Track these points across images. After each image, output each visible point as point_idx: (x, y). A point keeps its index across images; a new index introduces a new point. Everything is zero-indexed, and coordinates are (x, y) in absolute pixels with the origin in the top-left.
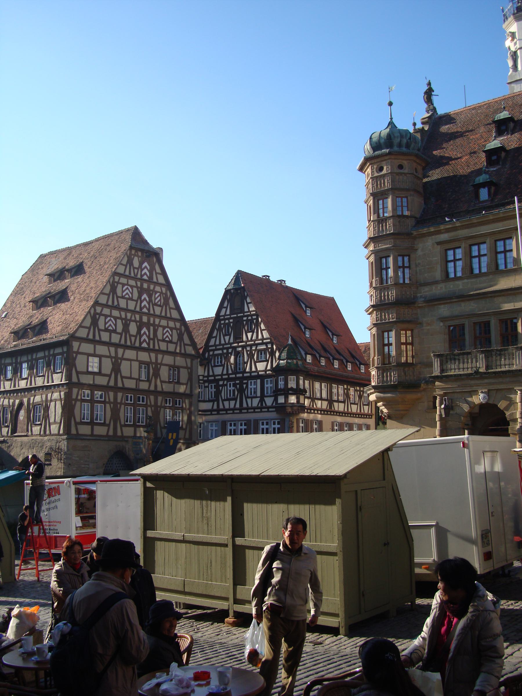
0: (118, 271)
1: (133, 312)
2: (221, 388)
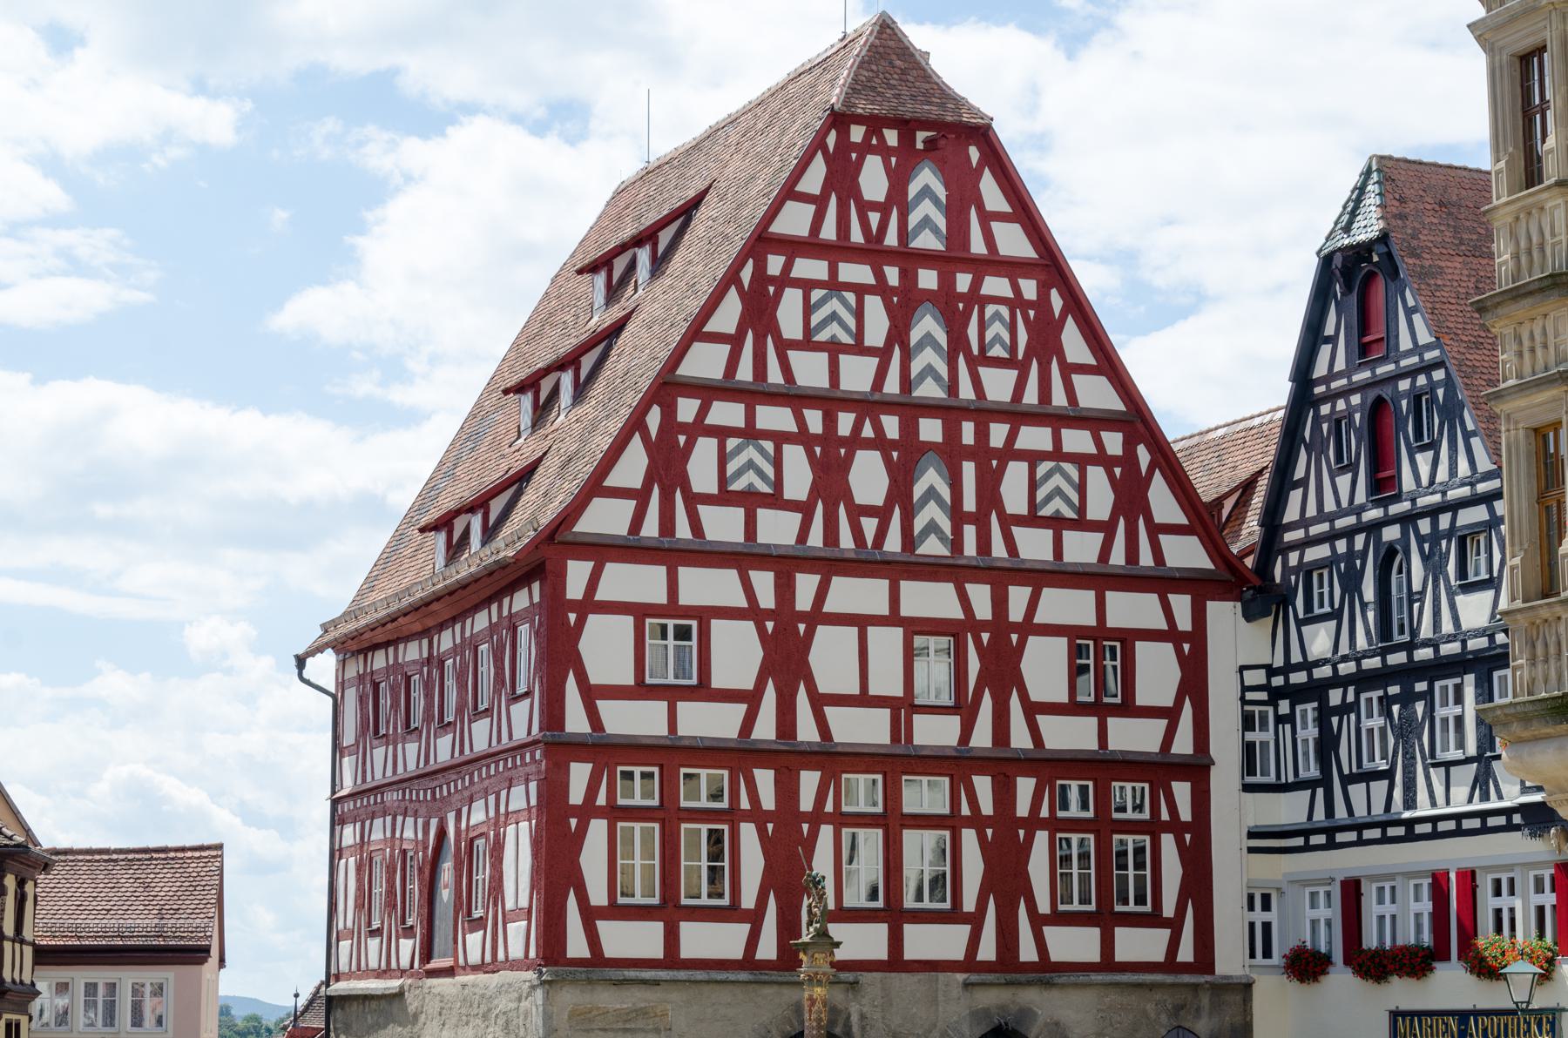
0: (779, 227)
1: (868, 406)
2: (1335, 720)
